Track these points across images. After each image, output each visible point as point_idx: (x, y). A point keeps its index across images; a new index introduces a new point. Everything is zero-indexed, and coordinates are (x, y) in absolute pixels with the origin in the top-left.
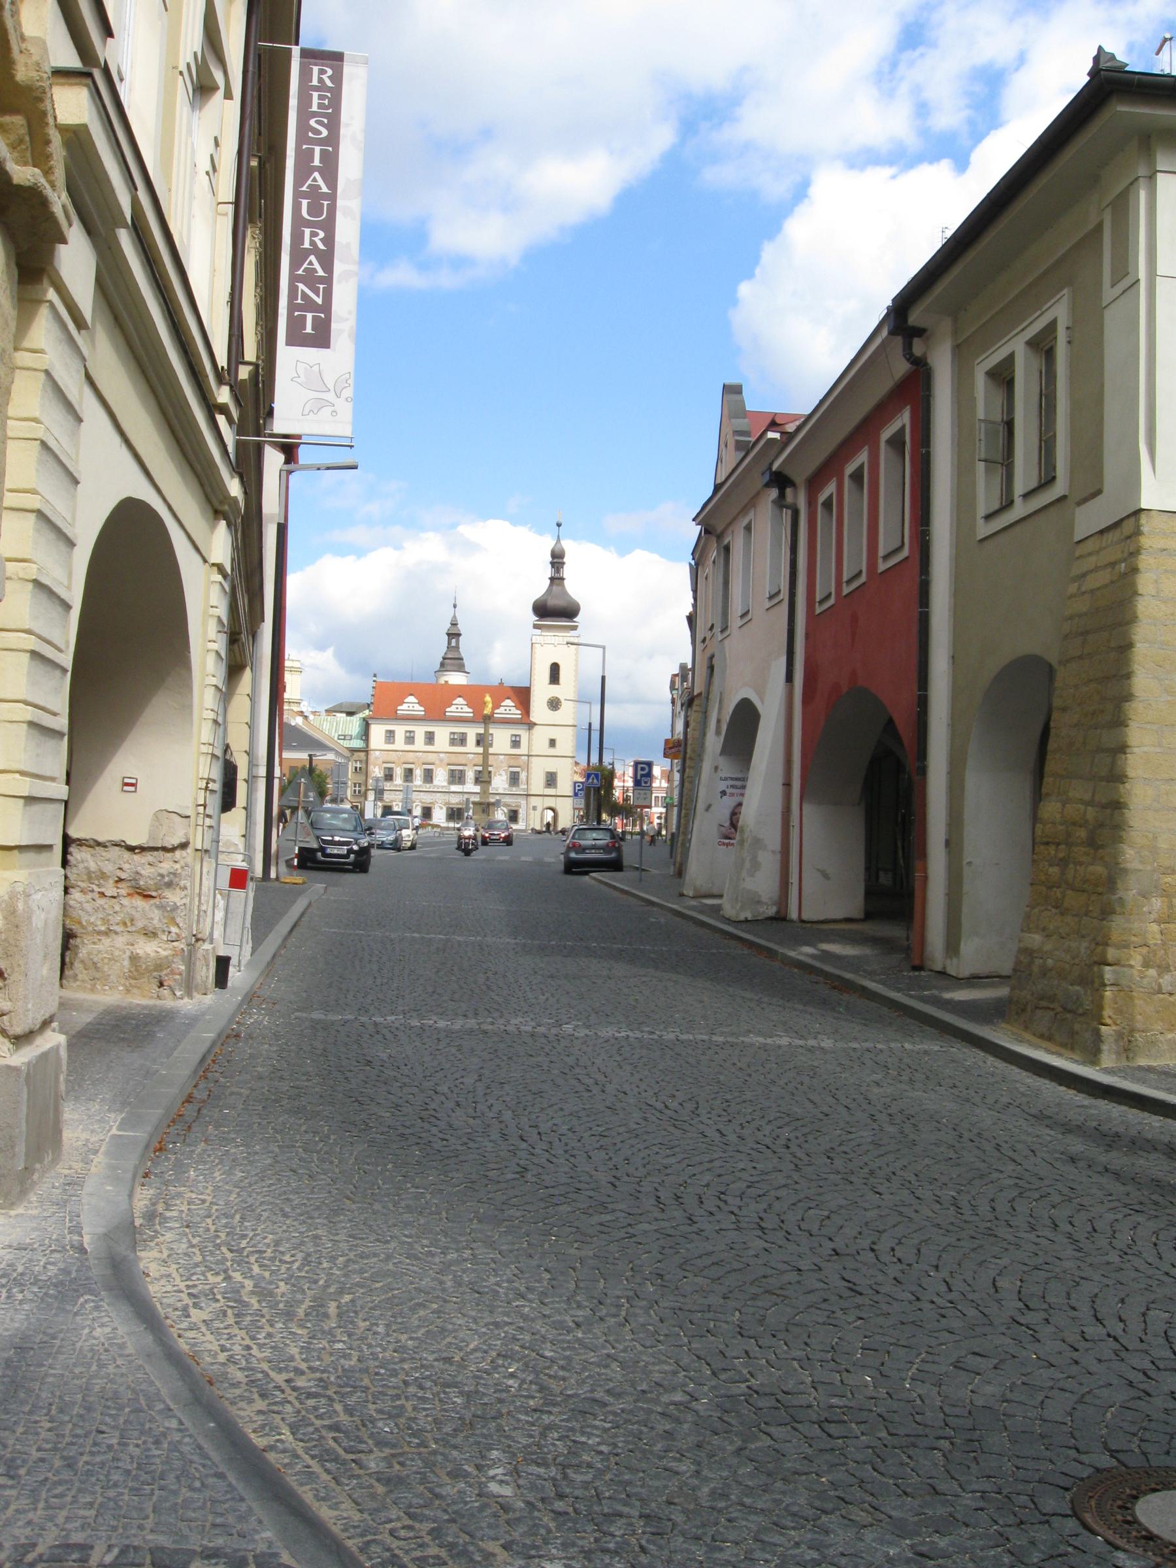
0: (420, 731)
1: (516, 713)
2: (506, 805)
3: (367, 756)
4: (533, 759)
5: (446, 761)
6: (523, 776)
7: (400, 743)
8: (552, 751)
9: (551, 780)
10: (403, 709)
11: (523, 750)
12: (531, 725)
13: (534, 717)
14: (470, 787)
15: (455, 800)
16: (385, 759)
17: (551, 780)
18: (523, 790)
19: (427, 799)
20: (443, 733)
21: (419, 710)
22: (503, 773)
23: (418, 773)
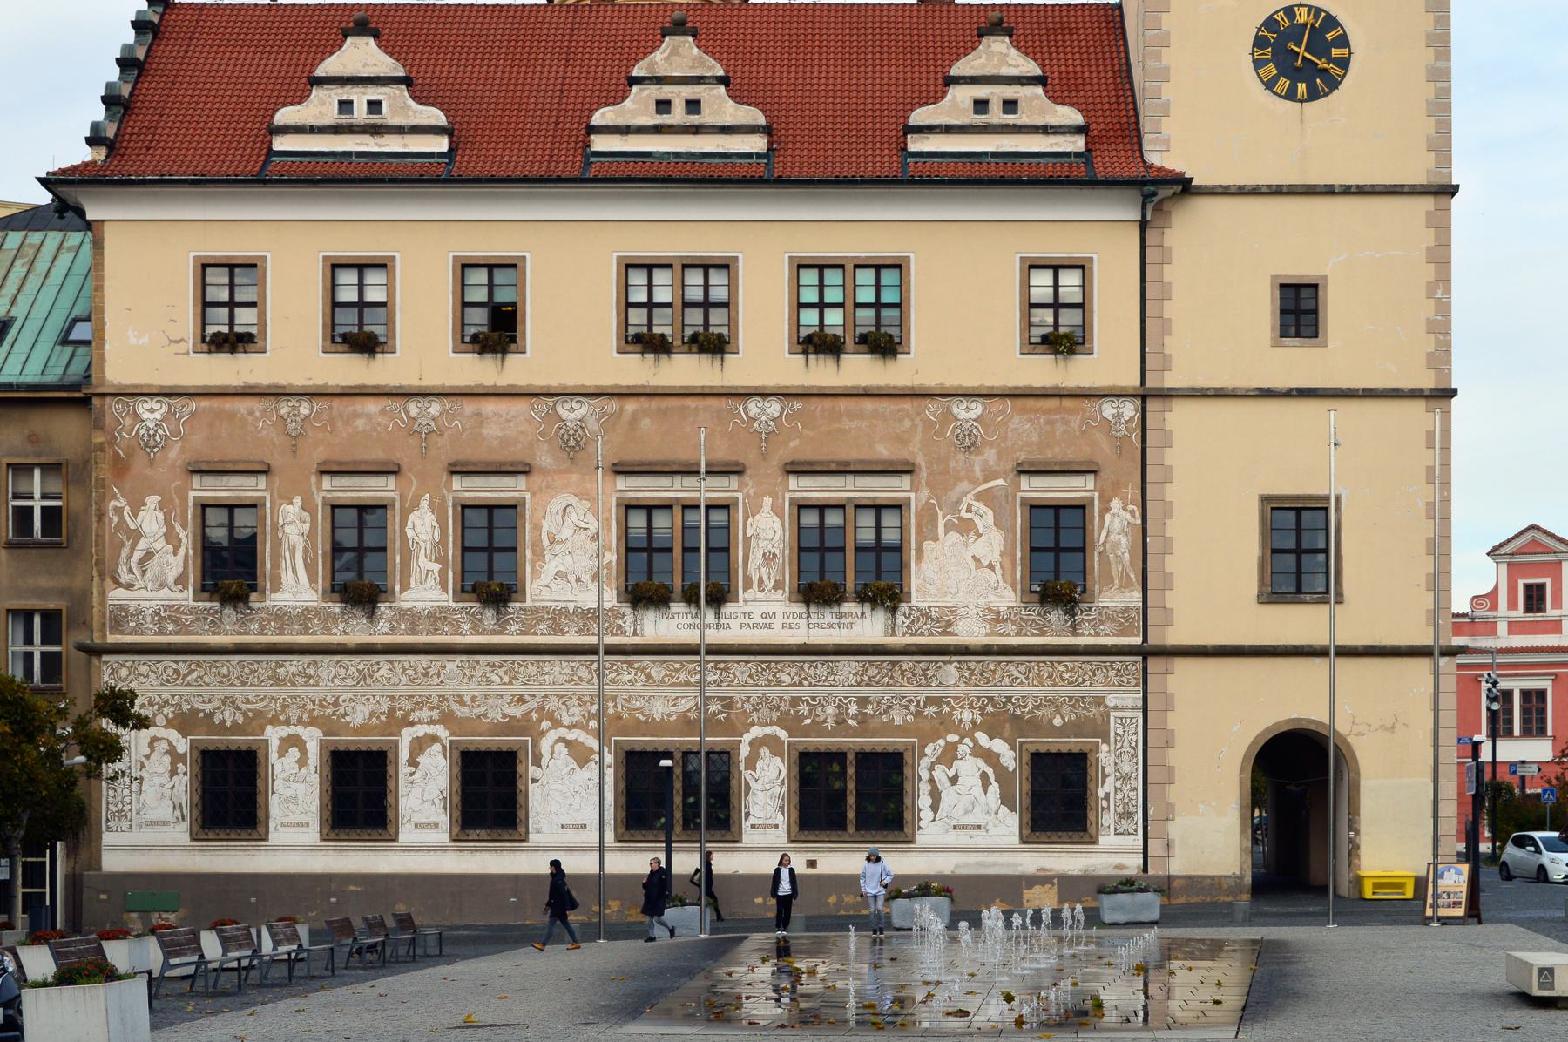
0: (424, 251)
1: (1051, 124)
2: (1000, 720)
3: (99, 425)
4: (1178, 419)
5: (601, 450)
6: (1113, 528)
7: (295, 348)
8: (1297, 364)
9: (1298, 547)
10: (308, 121)
11: (1109, 360)
12: (1162, 192)
13: (1170, 146)
14: (764, 611)
15: (662, 702)
16: (200, 445)
17: (1298, 547)
18: (1121, 619)
19: (487, 697)
20: (572, 259)
21: (416, 125)
22: (984, 518)
23: (423, 534)
